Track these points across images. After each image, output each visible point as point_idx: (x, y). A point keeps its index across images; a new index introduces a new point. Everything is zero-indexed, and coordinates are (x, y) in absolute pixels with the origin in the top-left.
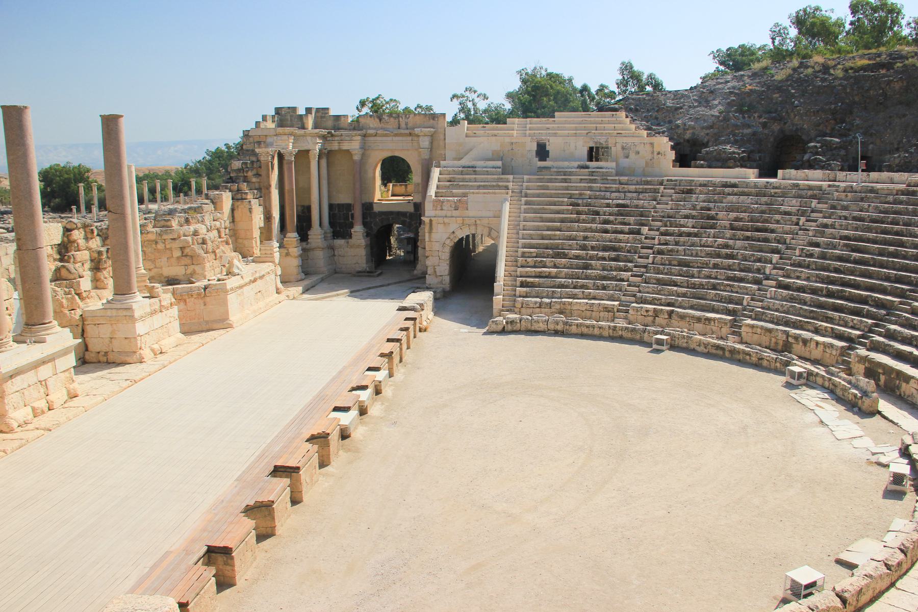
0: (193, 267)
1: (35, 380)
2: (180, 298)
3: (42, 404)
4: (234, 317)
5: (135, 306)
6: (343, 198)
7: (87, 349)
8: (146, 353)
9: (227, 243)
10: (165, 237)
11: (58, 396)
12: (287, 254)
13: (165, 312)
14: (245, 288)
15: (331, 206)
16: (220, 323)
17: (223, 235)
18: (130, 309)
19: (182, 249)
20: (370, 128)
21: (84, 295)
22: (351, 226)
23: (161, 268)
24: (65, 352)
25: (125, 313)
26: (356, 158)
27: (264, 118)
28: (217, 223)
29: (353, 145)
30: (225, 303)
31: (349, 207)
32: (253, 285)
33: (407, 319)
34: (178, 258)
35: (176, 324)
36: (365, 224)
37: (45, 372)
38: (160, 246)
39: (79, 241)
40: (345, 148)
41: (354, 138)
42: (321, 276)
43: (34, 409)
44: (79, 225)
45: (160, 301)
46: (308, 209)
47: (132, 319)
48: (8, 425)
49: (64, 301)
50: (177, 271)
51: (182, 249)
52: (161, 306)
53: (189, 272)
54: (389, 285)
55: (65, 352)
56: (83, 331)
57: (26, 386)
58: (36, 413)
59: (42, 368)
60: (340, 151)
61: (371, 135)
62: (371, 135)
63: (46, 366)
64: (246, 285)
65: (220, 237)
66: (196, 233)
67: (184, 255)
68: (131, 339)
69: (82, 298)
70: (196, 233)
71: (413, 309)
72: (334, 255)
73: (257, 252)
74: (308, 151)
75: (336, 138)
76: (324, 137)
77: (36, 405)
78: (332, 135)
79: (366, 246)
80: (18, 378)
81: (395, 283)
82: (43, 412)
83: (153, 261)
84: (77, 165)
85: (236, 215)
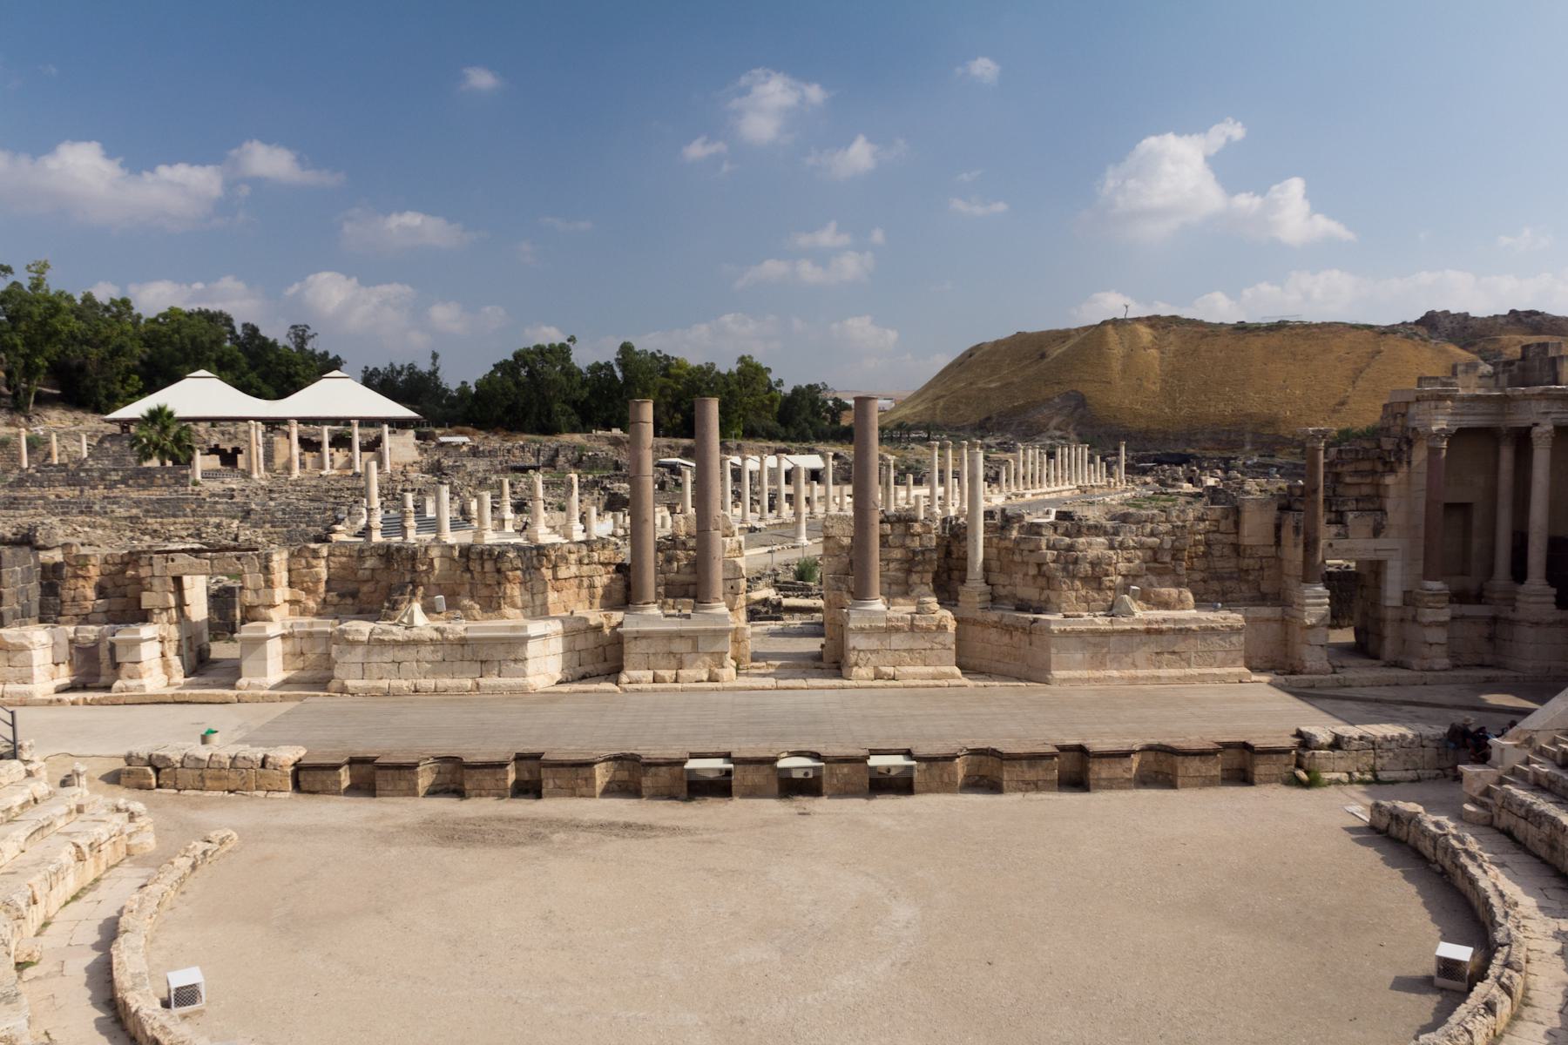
0: (1047, 592)
10: (1022, 546)
14: (1112, 639)
30: (1046, 649)
34: (1034, 577)
38: (1017, 558)
50: (1030, 593)
51: (1039, 565)
65: (1156, 561)
67: (1041, 574)
82: (664, 681)
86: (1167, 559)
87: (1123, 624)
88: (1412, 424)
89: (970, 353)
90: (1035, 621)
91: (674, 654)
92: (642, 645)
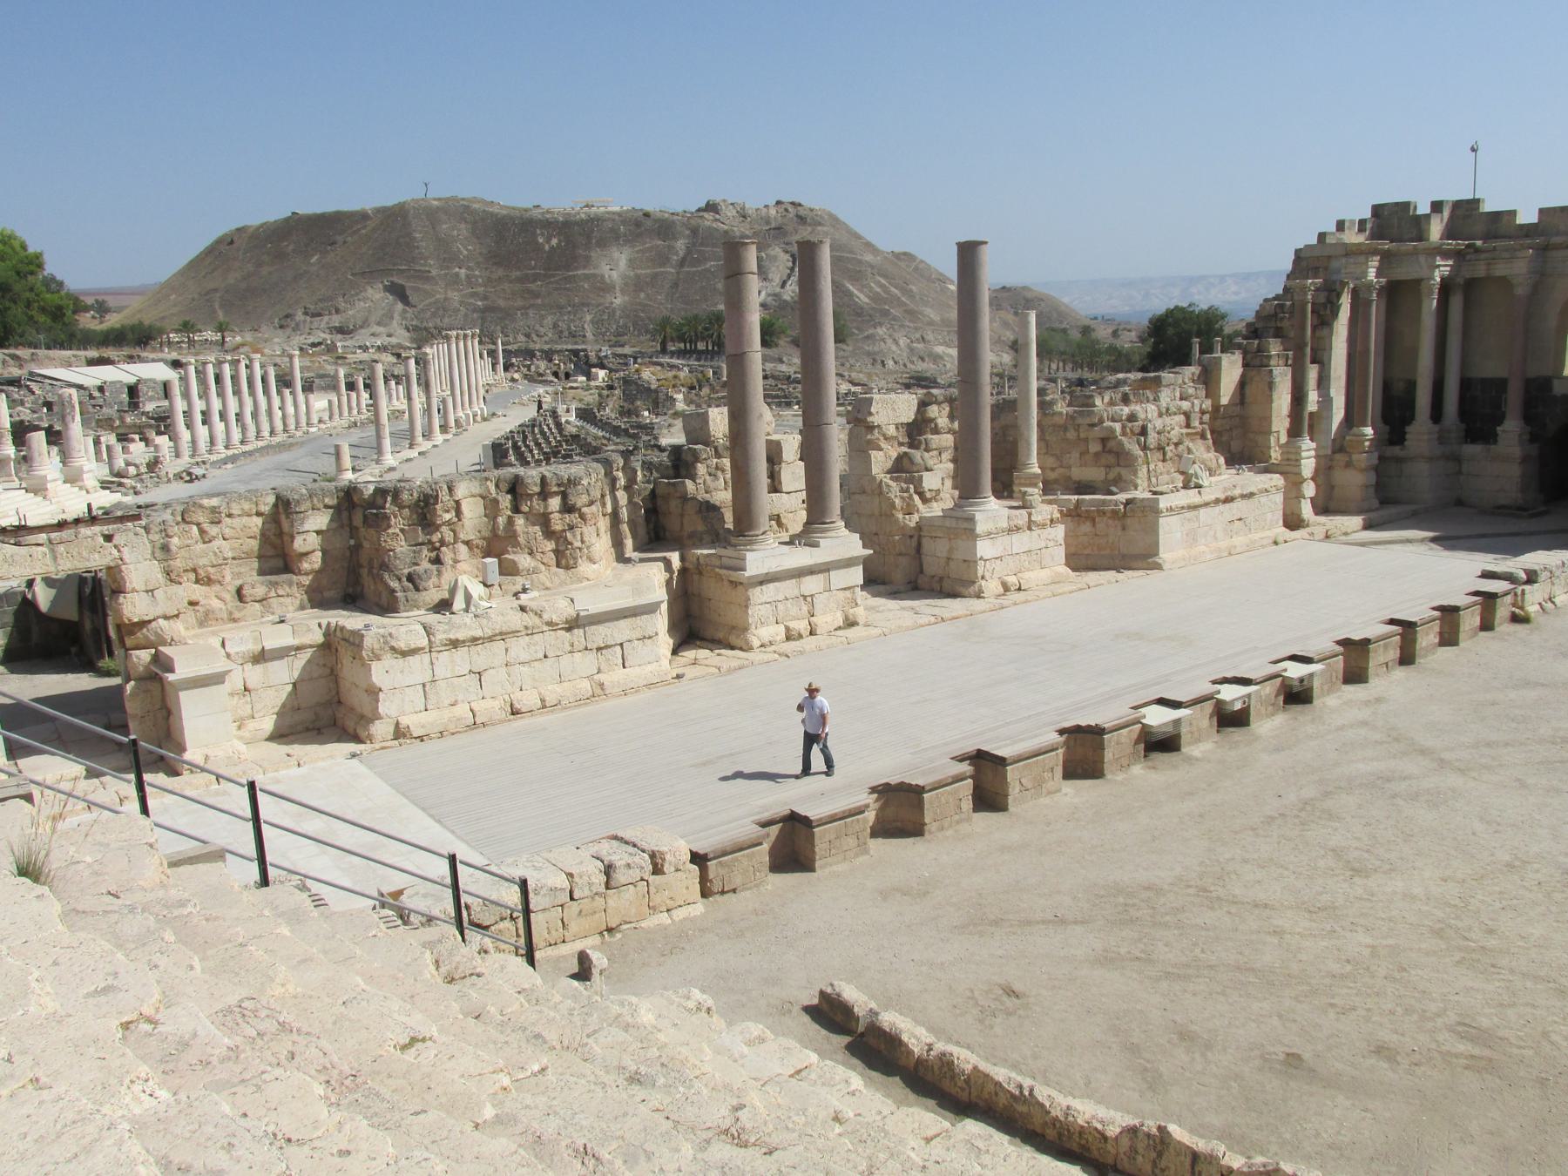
0: (1117, 470)
1: (796, 592)
2: (1073, 515)
3: (801, 626)
4: (1165, 555)
5: (978, 516)
6: (1490, 368)
7: (922, 572)
8: (991, 586)
9: (1203, 437)
10: (1080, 421)
11: (828, 618)
12: (1348, 465)
13: (1036, 532)
14: (1202, 511)
15: (1466, 384)
16: (1142, 557)
17: (1196, 423)
18: (971, 520)
19: (1104, 441)
20: (1558, 234)
21: (928, 495)
22: (1499, 419)
23: (1069, 467)
24: (848, 563)
25: (966, 525)
26: (1520, 291)
27: (1341, 226)
28: (1185, 405)
29: (1517, 268)
30: (1154, 530)
31: (1501, 384)
32: (1221, 507)
33: (1476, 593)
34: (1097, 454)
35: (1060, 553)
36: (1528, 417)
37: (812, 584)
38: (1071, 435)
39: (939, 421)
40: (1498, 273)
41: (1518, 254)
42: (1413, 507)
43: (788, 629)
44: (941, 398)
45: (1030, 515)
46: (1411, 386)
47: (971, 534)
48: (747, 642)
49: (897, 501)
50: (1094, 474)
51: (1104, 441)
52: (1030, 521)
53: (1111, 476)
54: (1531, 534)
55: (848, 563)
56: (919, 545)
57: (781, 597)
58: (790, 636)
59: (808, 578)
60: (1489, 279)
61: (1557, 247)
62: (1557, 247)
63: (814, 577)
64: (1206, 504)
65: (1188, 426)
66: (1132, 418)
68: (971, 562)
69: (925, 500)
70: (1132, 418)
71: (1509, 577)
72: (1460, 473)
73: (1275, 455)
74: (1418, 282)
75: (1483, 256)
76: (1458, 255)
77: (792, 625)
78: (1477, 250)
79: (1525, 459)
80: (771, 586)
81: (1545, 532)
82: (800, 636)
83: (1058, 458)
84: (1205, 307)
85: (1248, 391)
86: (1196, 423)
87: (1208, 496)
88: (1335, 277)
89: (228, 241)
90: (1128, 502)
91: (805, 597)
92: (770, 591)
